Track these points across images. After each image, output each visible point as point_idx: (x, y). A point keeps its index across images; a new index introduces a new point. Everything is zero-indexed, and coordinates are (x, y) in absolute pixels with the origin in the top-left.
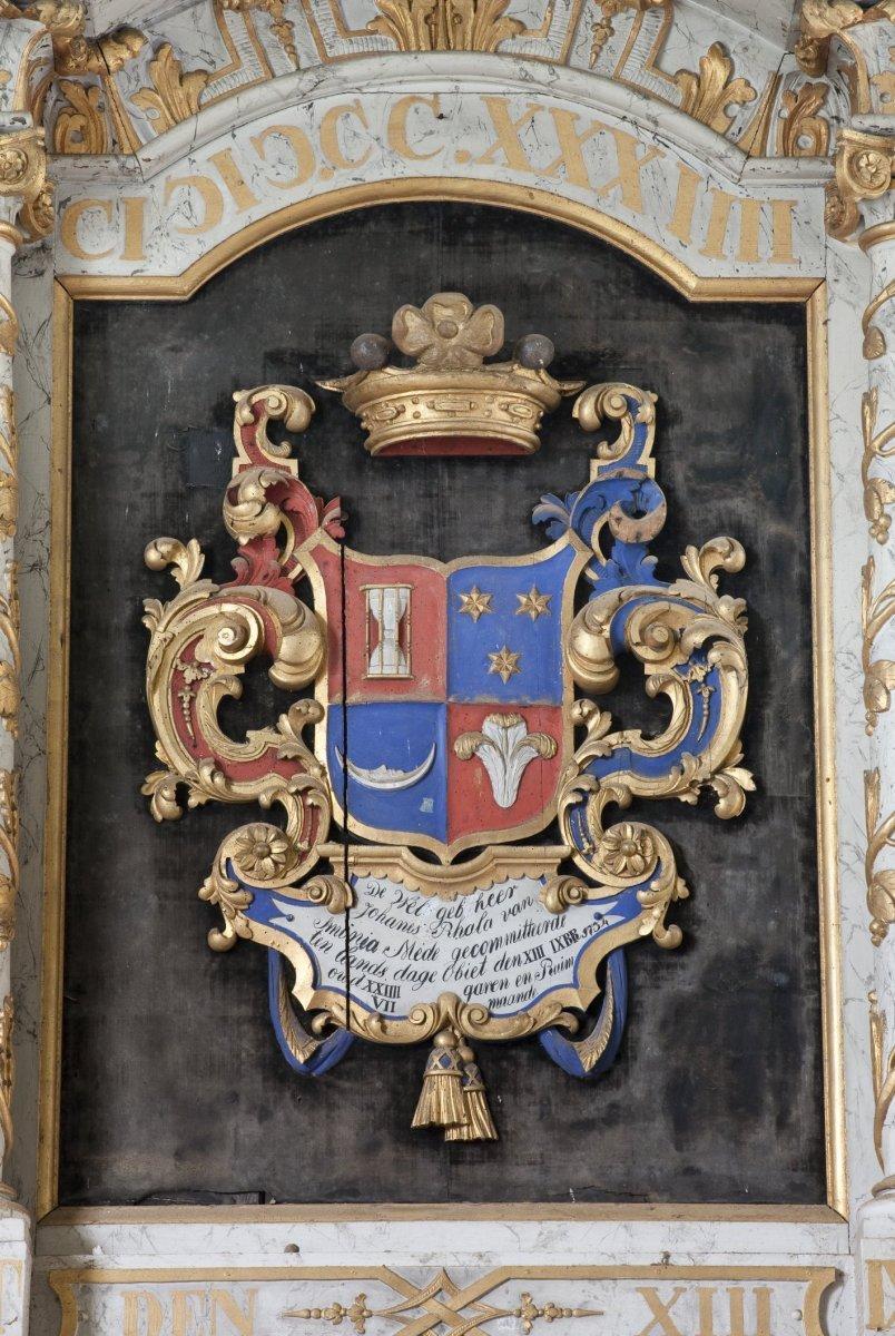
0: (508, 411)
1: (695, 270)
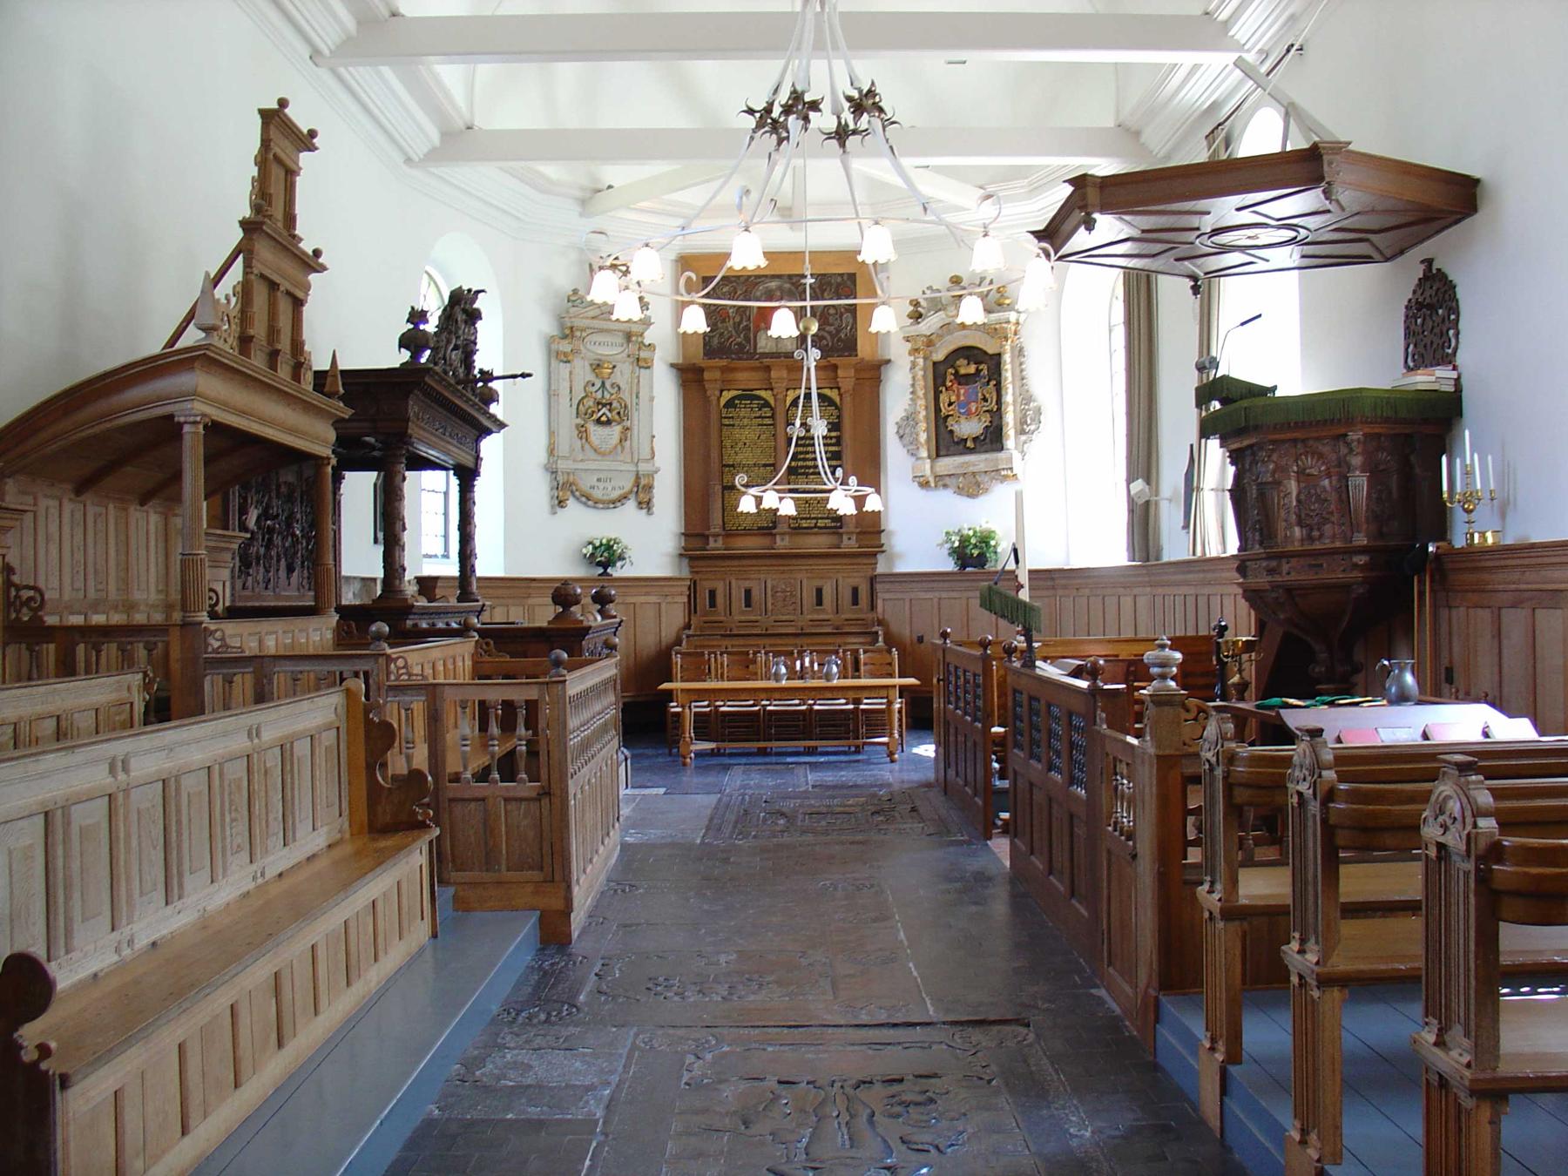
0: (972, 369)
1: (990, 352)
